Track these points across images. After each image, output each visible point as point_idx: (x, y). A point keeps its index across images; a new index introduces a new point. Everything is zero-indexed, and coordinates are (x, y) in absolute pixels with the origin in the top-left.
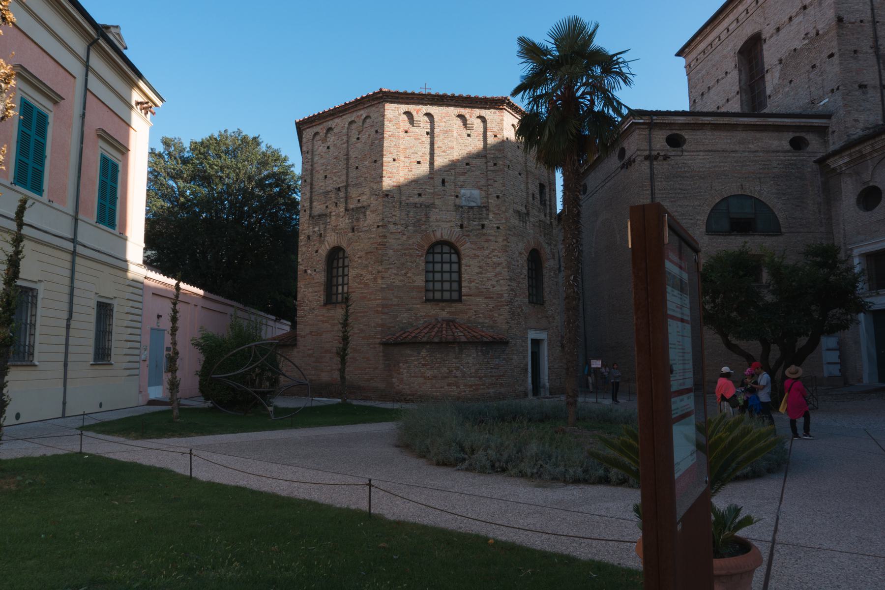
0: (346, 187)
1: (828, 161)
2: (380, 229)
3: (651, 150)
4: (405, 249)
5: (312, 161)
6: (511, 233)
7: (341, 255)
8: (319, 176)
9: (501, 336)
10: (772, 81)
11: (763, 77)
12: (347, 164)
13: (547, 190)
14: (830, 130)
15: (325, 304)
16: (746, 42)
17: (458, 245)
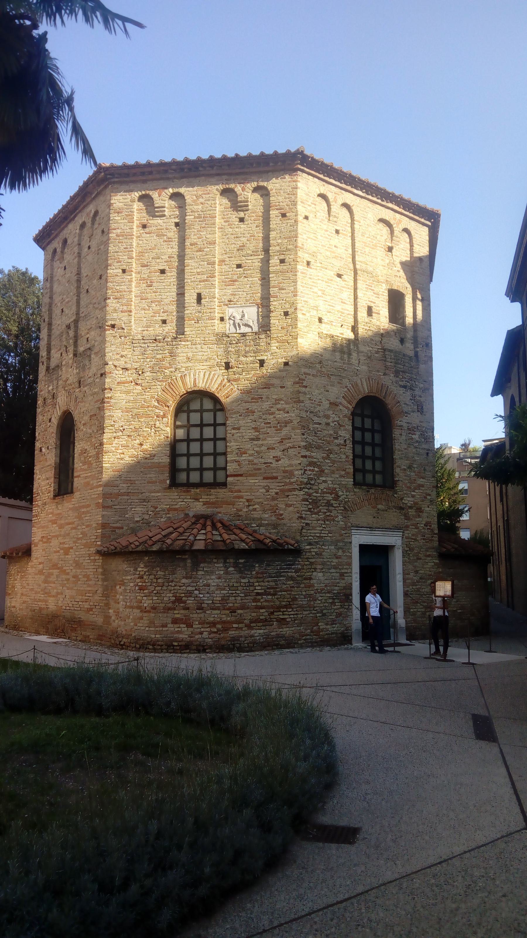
0: (76, 322)
4: (138, 409)
8: (57, 311)
15: (55, 496)
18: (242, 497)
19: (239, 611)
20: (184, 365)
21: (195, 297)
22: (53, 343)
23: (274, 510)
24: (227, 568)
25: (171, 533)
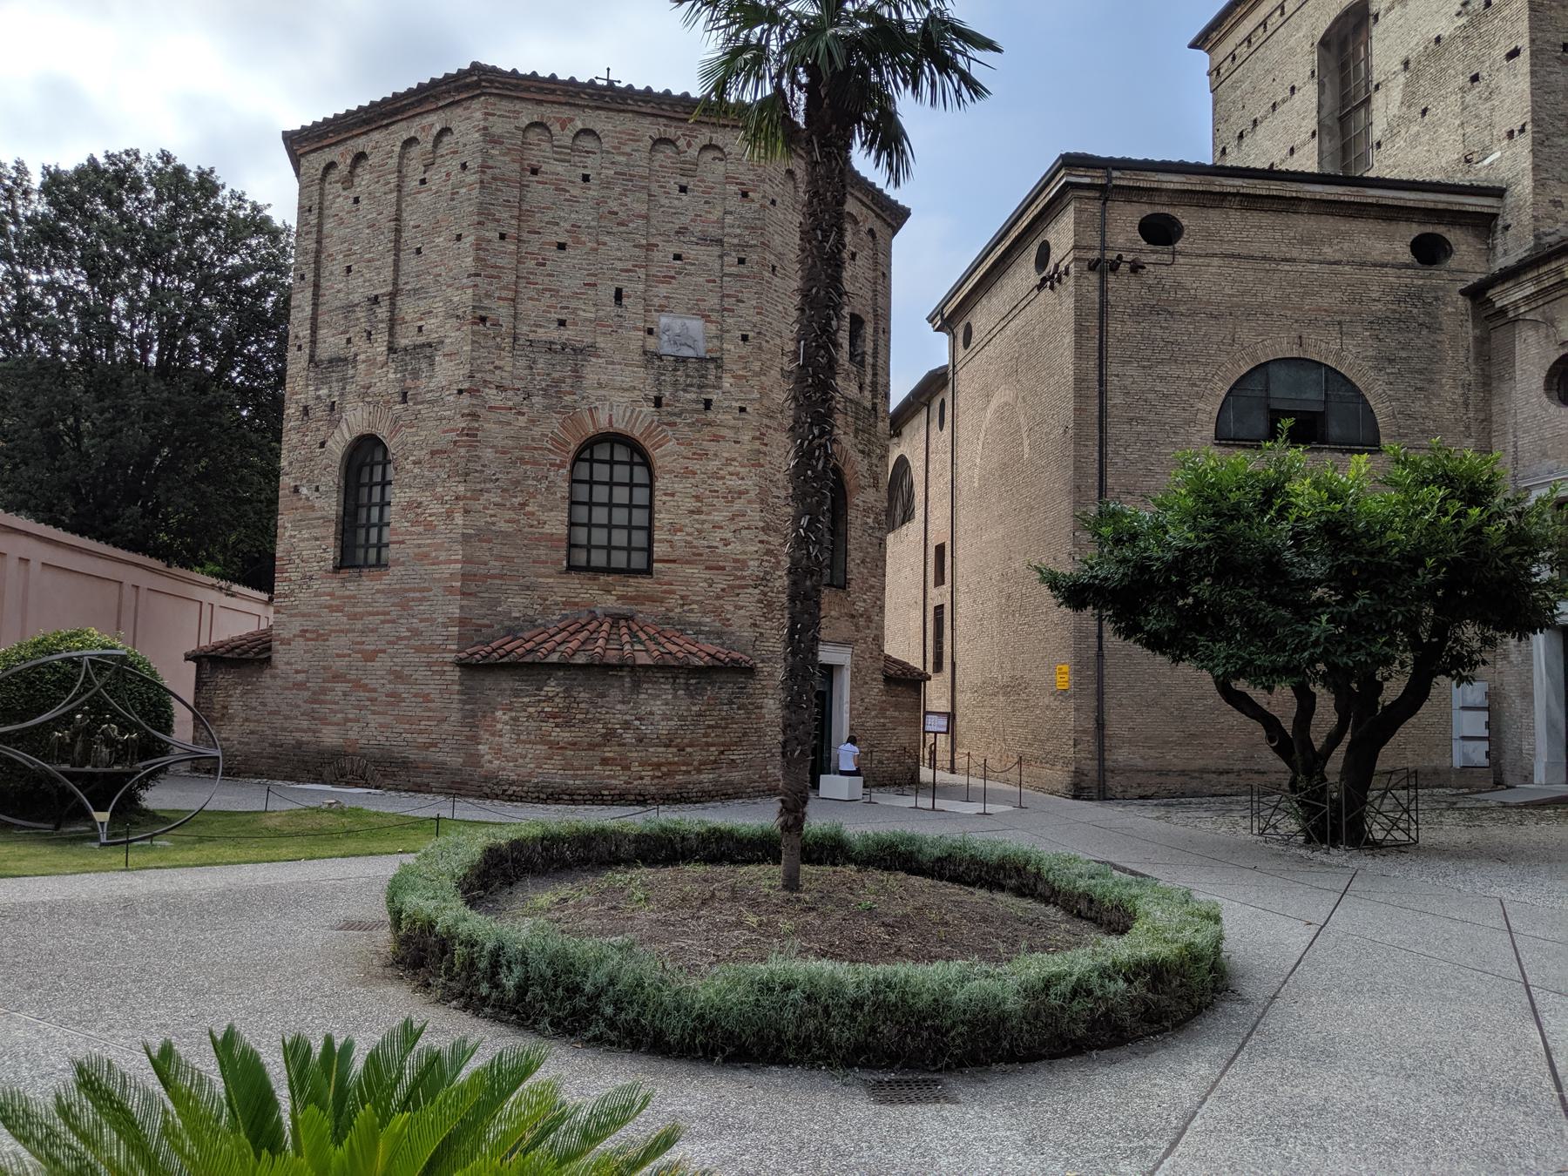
0: (393, 295)
1: (1490, 293)
2: (465, 399)
3: (1104, 248)
4: (521, 449)
5: (320, 231)
6: (774, 424)
7: (379, 457)
8: (334, 267)
9: (736, 655)
10: (1385, 110)
11: (1368, 101)
12: (397, 241)
13: (869, 330)
14: (1500, 222)
15: (337, 569)
16: (1338, 20)
17: (647, 444)
18: (673, 592)
19: (689, 750)
21: (613, 293)
22: (320, 319)
23: (718, 612)
24: (676, 690)
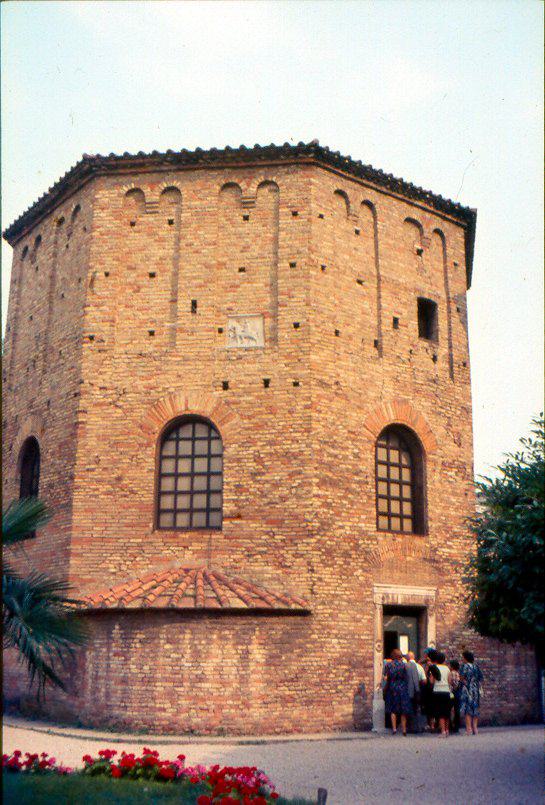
4: (117, 436)
5: (19, 296)
20: (173, 385)
25: (154, 587)
